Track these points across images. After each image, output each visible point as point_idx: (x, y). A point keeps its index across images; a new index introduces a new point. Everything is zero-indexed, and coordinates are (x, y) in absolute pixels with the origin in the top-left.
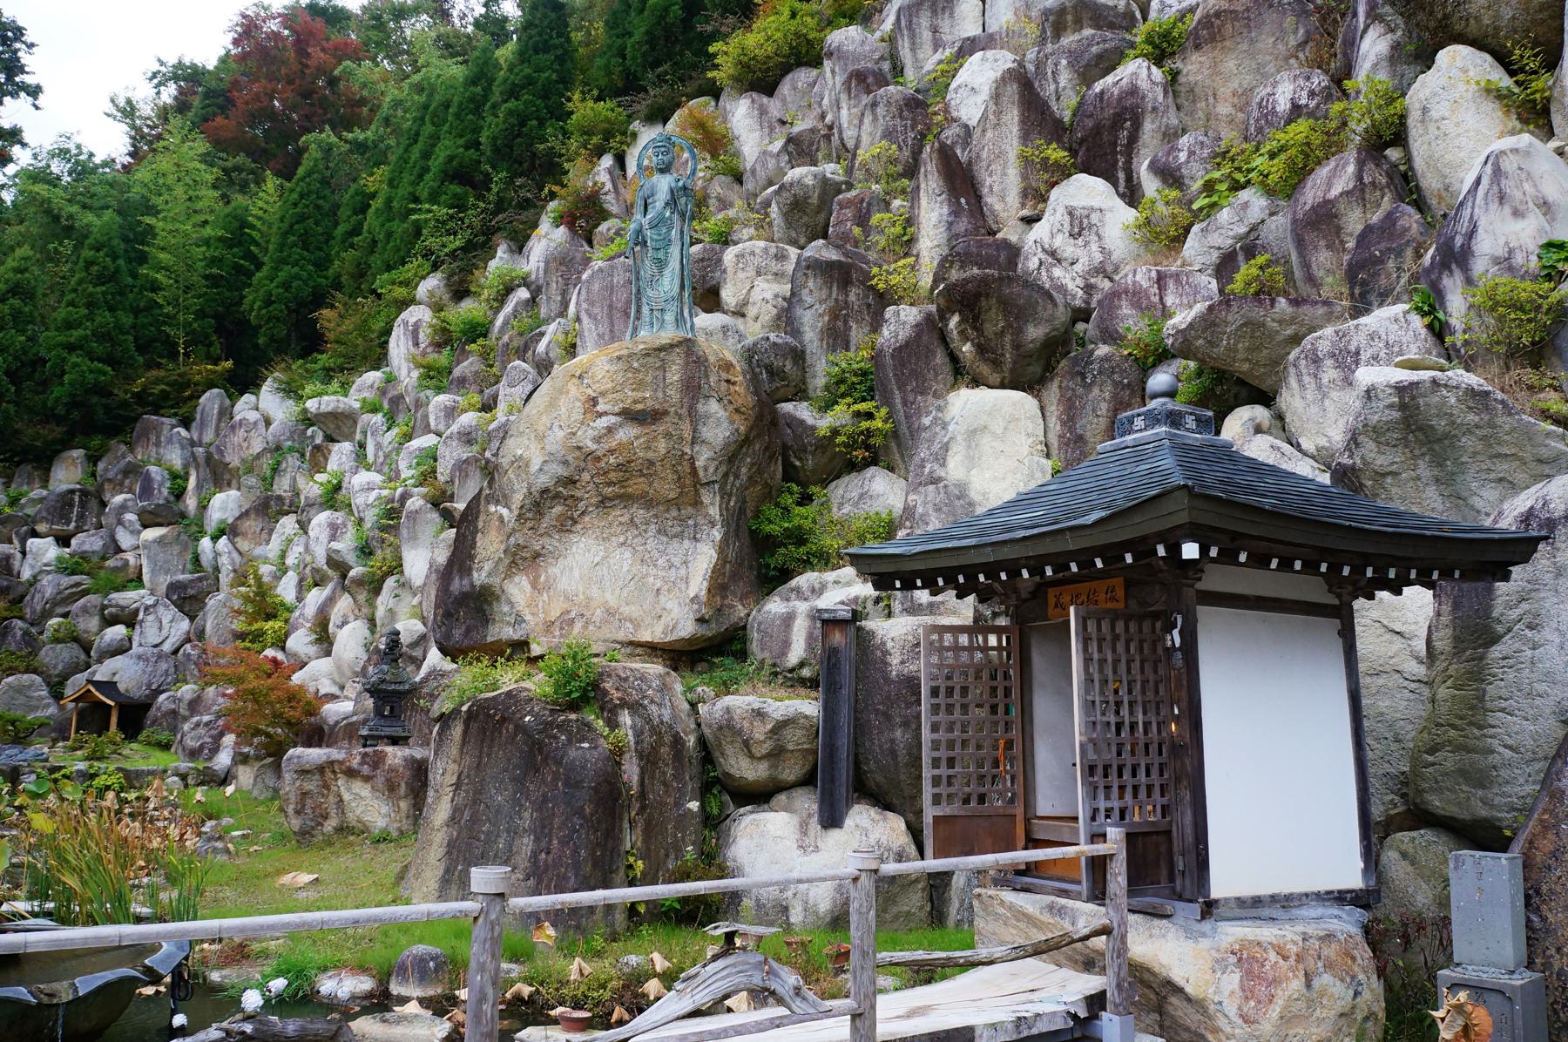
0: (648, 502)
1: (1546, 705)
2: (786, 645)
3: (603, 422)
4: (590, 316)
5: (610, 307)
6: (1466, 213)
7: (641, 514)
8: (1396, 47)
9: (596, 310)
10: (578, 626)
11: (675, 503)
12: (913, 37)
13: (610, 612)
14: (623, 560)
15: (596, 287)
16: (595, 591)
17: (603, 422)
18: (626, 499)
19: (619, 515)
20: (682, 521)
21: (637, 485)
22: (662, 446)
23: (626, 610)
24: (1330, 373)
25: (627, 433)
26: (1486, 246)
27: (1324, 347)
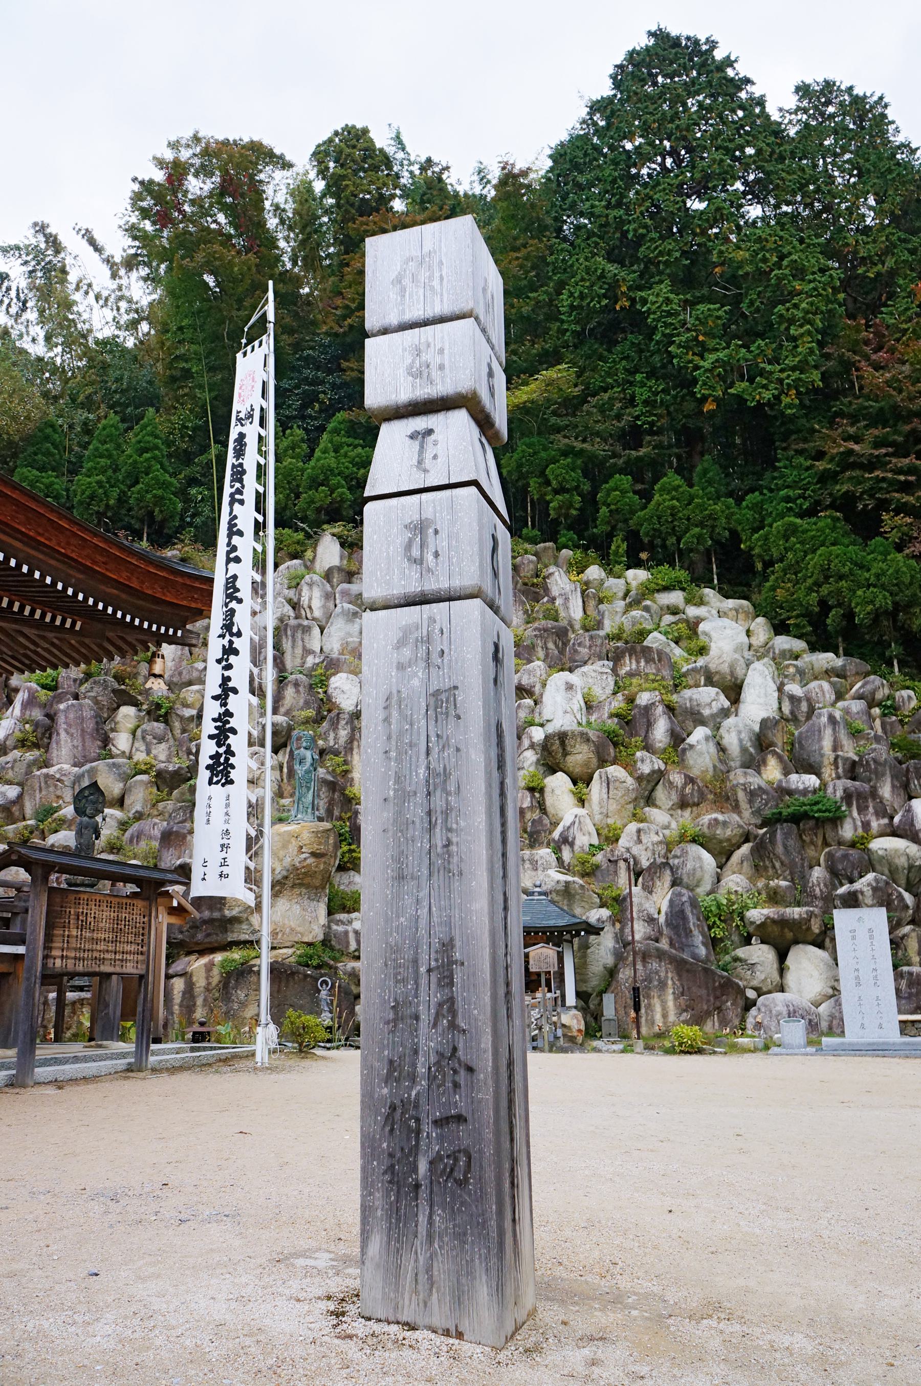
0: (307, 886)
1: (601, 964)
2: (348, 943)
3: (304, 856)
4: (68, 733)
5: (83, 730)
6: (571, 830)
7: (304, 890)
8: (538, 760)
9: (73, 731)
10: (280, 936)
11: (317, 888)
12: (294, 641)
13: (292, 930)
14: (297, 909)
15: (71, 716)
16: (286, 922)
17: (304, 856)
18: (301, 885)
19: (297, 891)
20: (316, 894)
21: (307, 880)
22: (322, 867)
23: (298, 929)
24: (527, 865)
25: (311, 861)
26: (578, 843)
27: (526, 857)
